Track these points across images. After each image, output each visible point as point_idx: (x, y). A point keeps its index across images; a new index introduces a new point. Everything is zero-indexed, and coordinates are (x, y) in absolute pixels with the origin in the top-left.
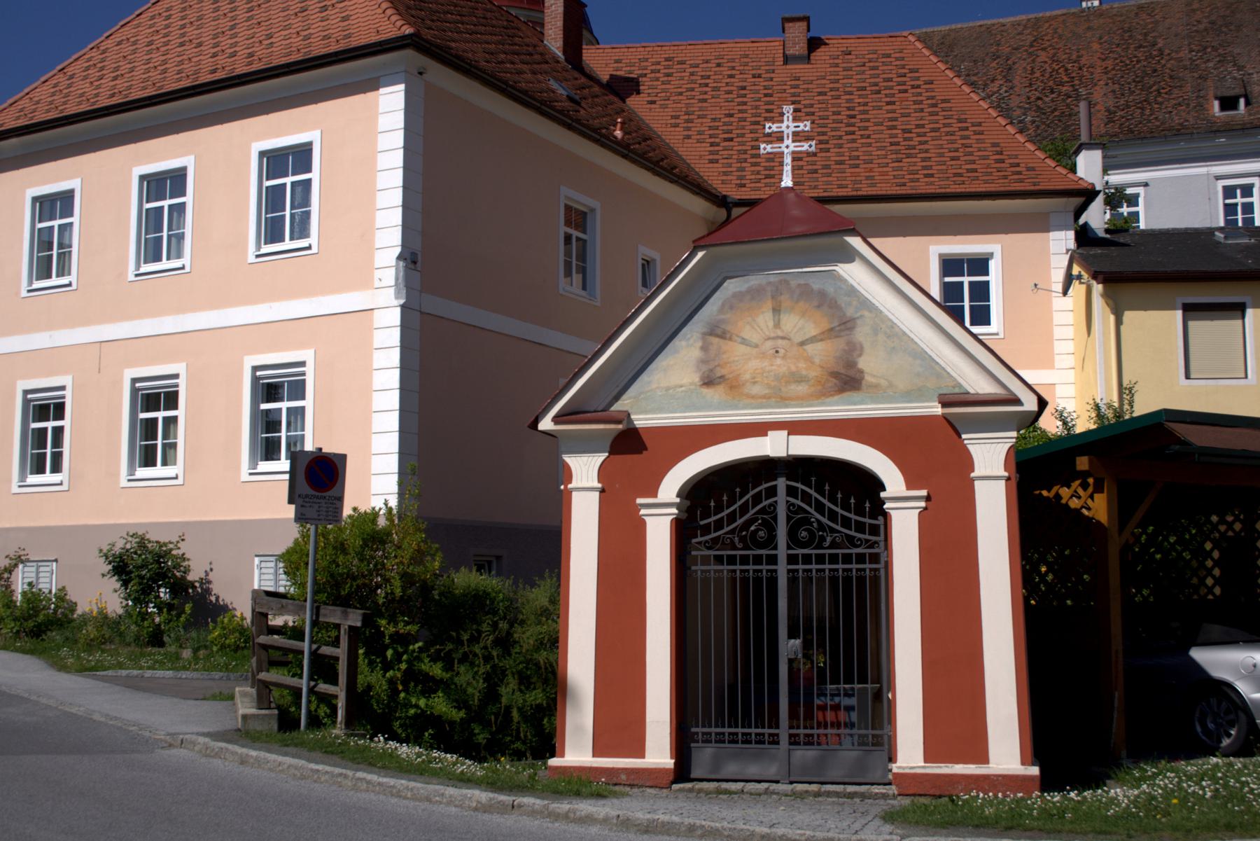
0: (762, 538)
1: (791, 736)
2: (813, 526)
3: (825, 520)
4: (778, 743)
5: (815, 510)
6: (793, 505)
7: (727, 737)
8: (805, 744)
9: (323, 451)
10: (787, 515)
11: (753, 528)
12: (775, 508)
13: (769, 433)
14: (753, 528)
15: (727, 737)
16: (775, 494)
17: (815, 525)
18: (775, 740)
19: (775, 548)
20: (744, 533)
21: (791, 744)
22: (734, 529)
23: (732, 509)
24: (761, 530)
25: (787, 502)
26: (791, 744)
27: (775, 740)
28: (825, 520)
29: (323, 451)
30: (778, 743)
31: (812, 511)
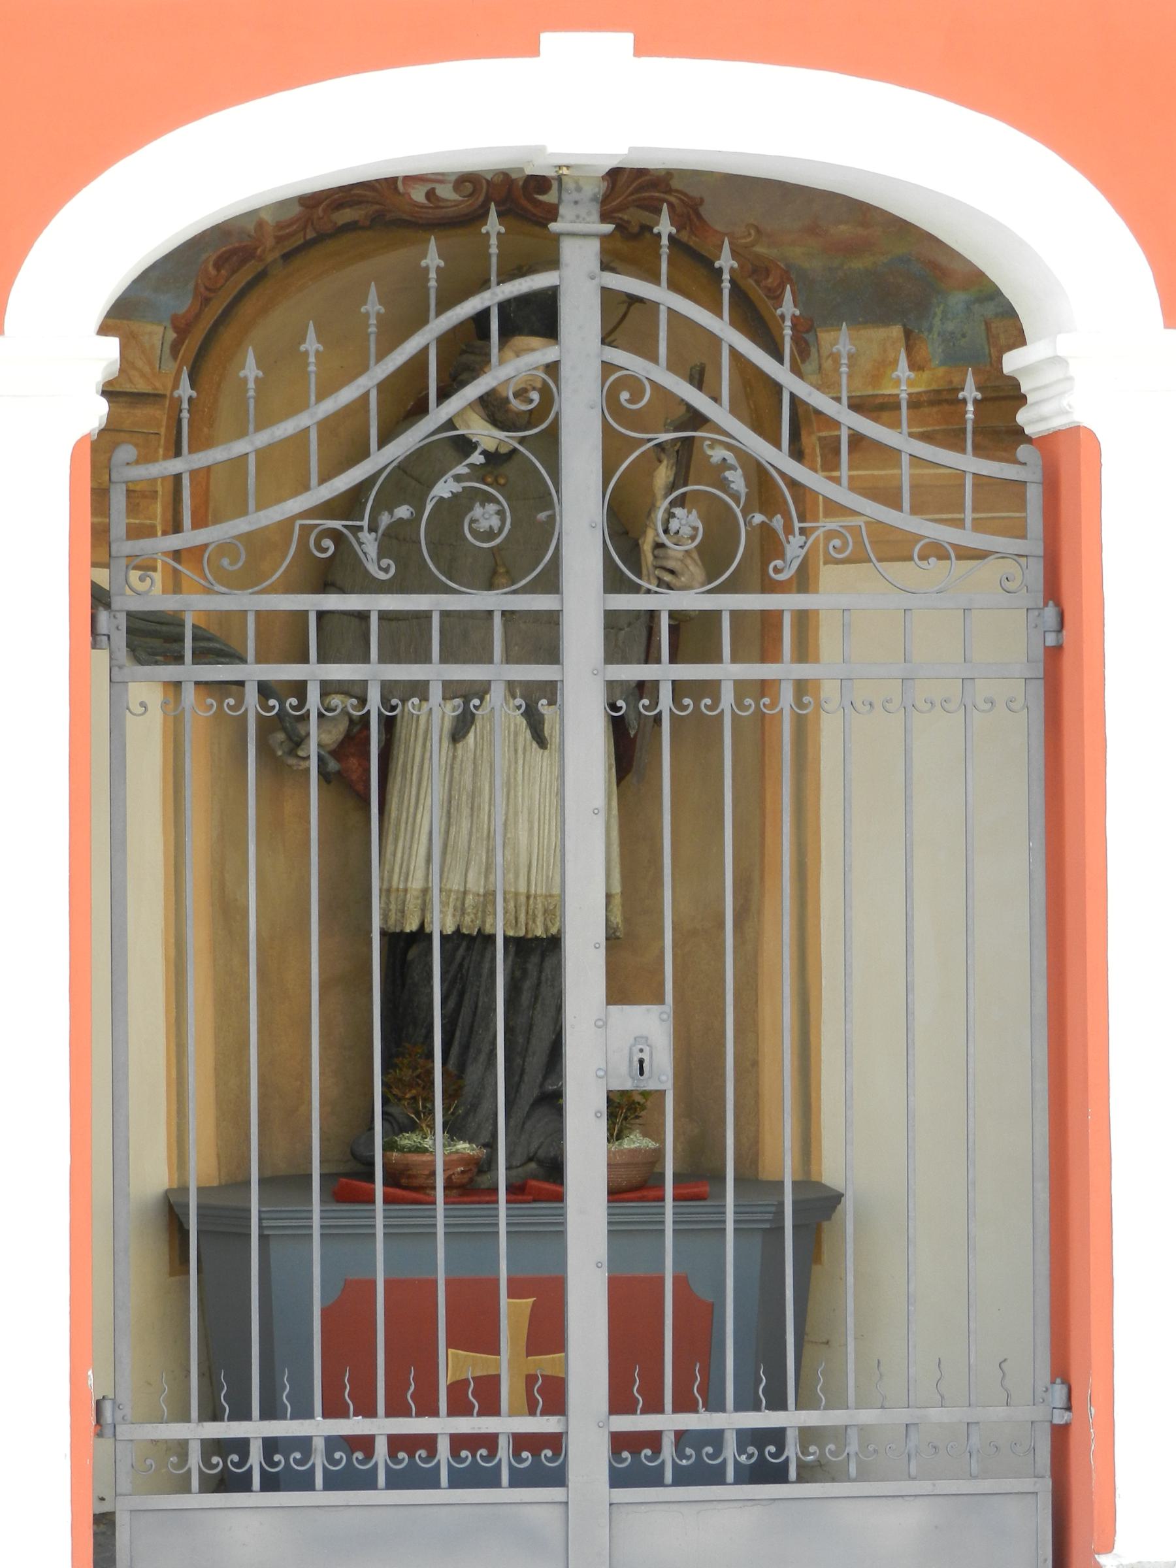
0: (490, 535)
1: (620, 1442)
2: (724, 485)
3: (777, 458)
4: (558, 1478)
5: (734, 411)
6: (633, 384)
7: (318, 1460)
8: (683, 1478)
9: (626, 39)
10: (606, 428)
11: (444, 488)
12: (548, 398)
13: (548, 39)
14: (444, 488)
15: (318, 1460)
16: (549, 328)
17: (737, 479)
18: (803, 618)
19: (550, 582)
20: (403, 512)
21: (618, 1479)
22: (358, 493)
23: (286, 428)
24: (488, 499)
25: (608, 367)
26: (618, 1479)
27: (803, 618)
28: (777, 458)
29: (626, 39)
30: (558, 1478)
31: (718, 413)
